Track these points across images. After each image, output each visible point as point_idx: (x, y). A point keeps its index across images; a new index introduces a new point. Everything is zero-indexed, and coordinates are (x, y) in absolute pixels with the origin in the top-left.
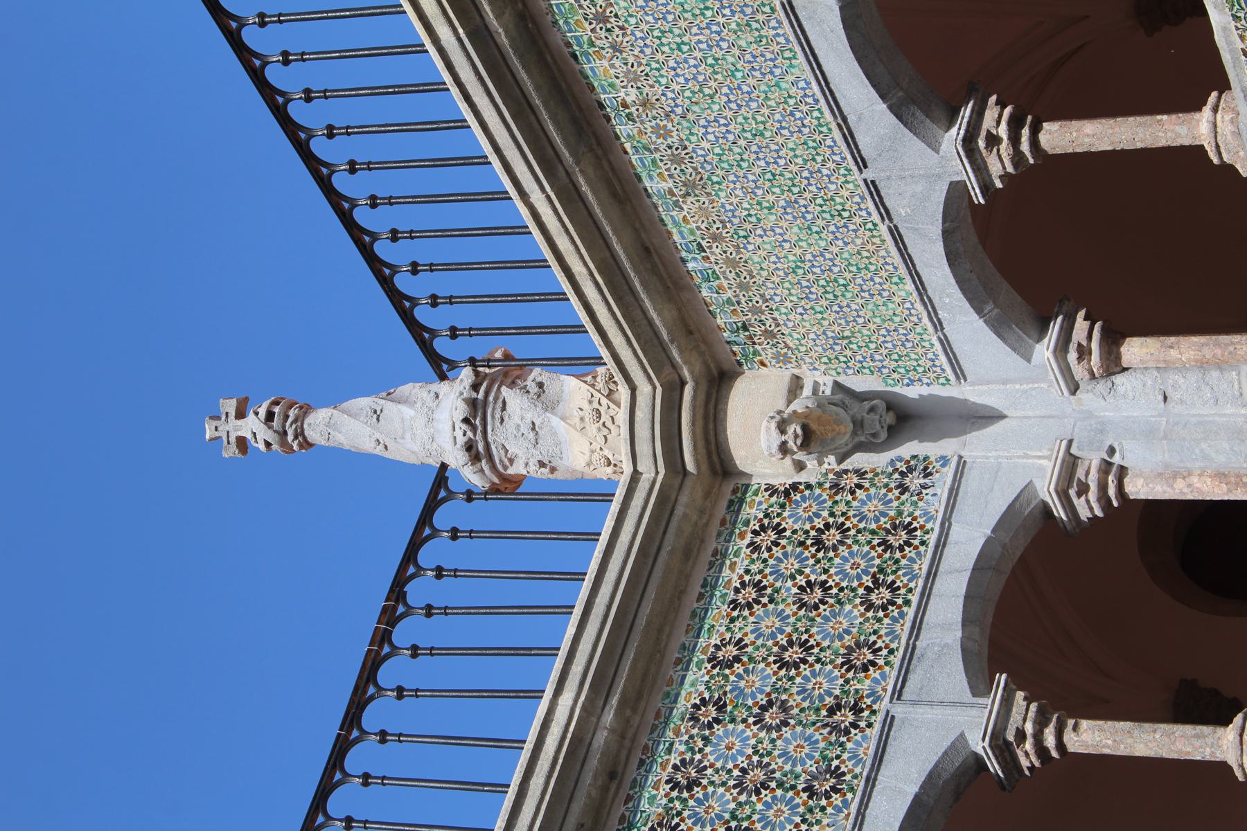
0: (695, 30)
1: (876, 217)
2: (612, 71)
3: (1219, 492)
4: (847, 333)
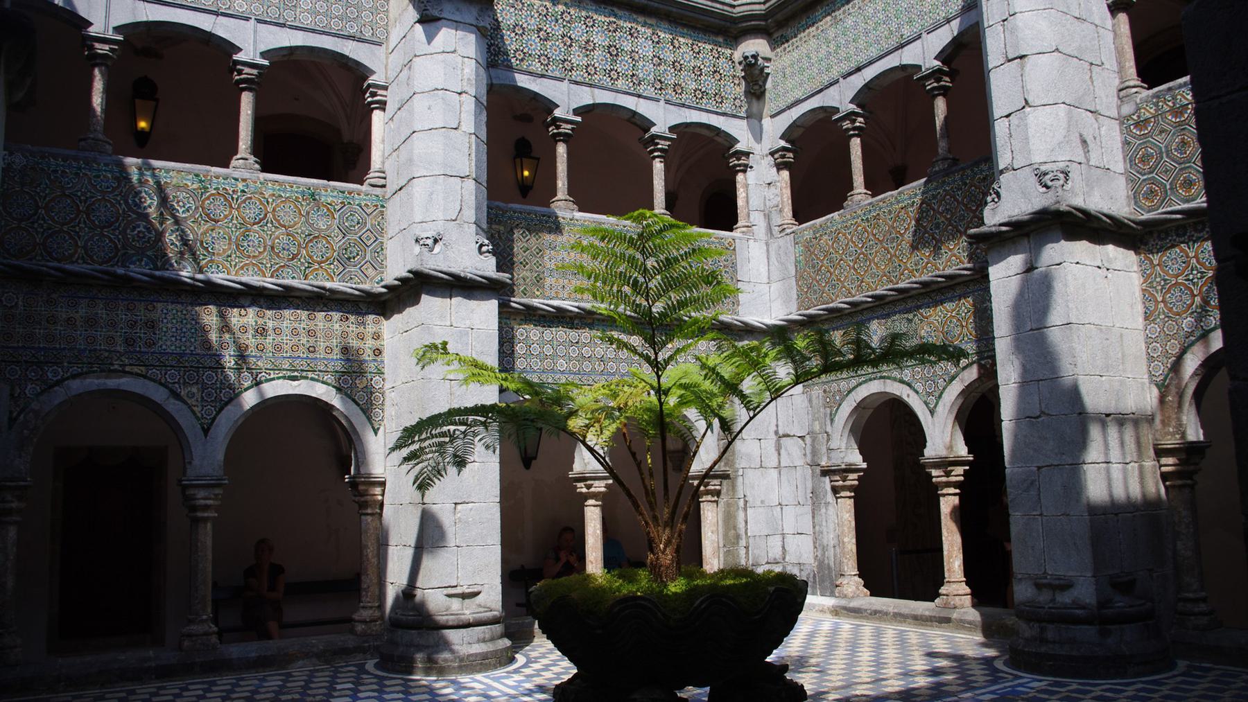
3: (740, 202)
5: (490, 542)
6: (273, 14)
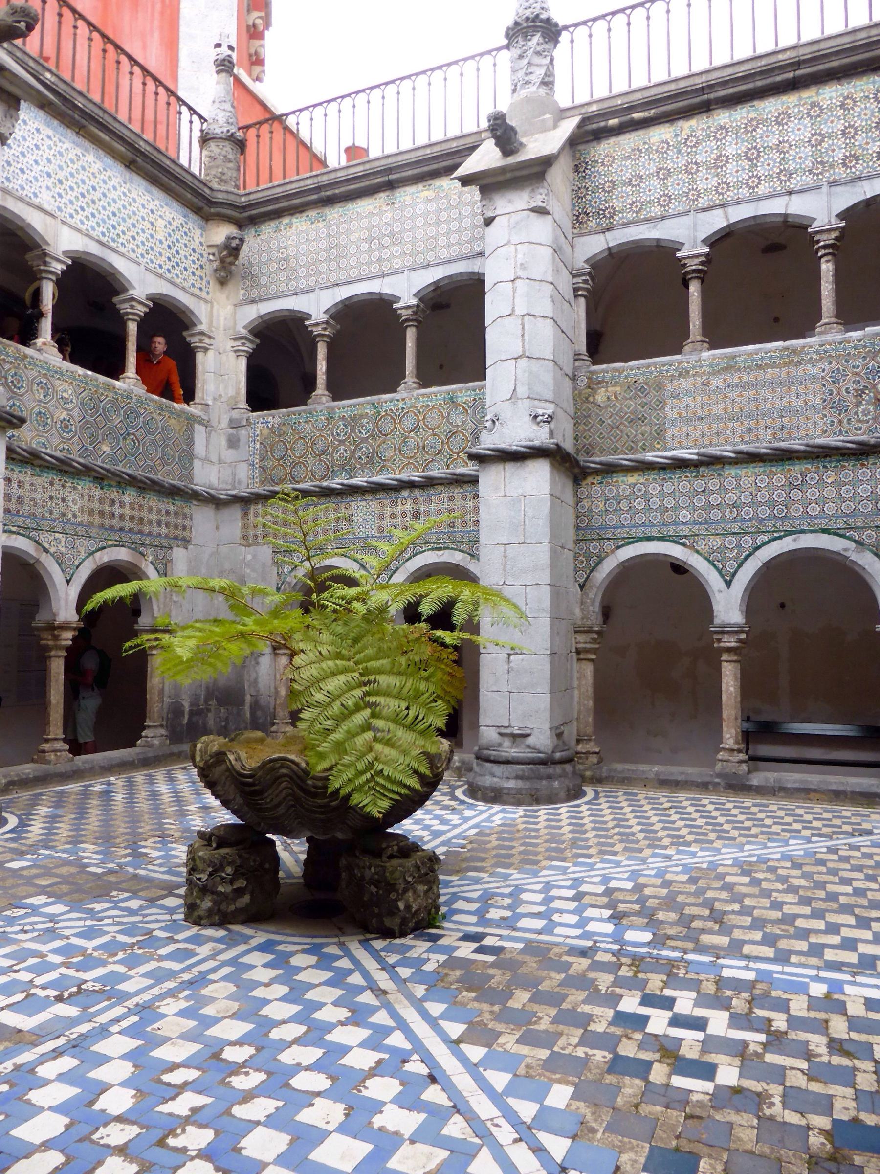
5: (539, 690)
6: (420, 259)
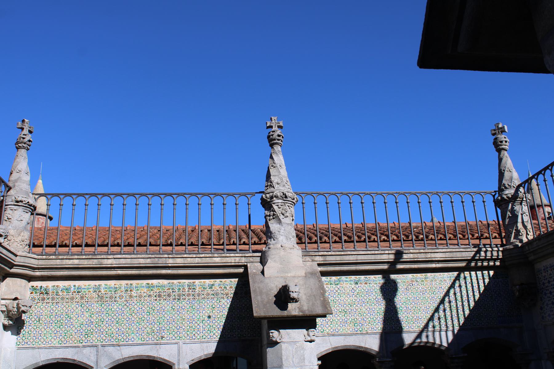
0: (153, 318)
1: (84, 344)
2: (142, 292)
4: (41, 322)
